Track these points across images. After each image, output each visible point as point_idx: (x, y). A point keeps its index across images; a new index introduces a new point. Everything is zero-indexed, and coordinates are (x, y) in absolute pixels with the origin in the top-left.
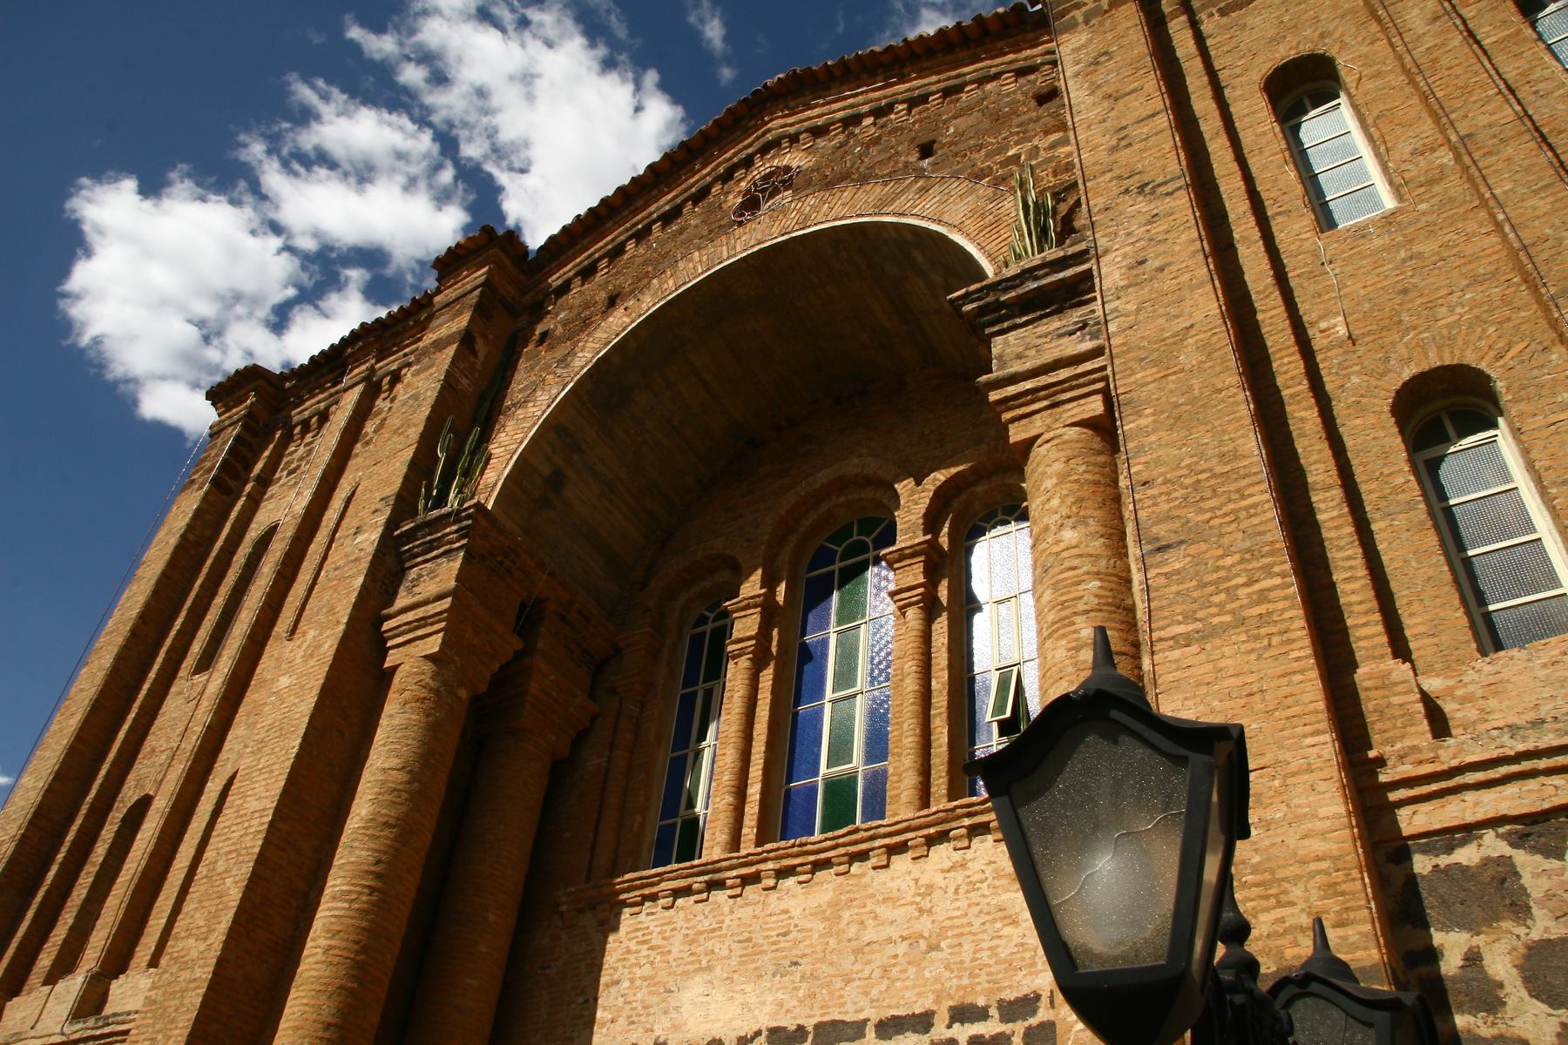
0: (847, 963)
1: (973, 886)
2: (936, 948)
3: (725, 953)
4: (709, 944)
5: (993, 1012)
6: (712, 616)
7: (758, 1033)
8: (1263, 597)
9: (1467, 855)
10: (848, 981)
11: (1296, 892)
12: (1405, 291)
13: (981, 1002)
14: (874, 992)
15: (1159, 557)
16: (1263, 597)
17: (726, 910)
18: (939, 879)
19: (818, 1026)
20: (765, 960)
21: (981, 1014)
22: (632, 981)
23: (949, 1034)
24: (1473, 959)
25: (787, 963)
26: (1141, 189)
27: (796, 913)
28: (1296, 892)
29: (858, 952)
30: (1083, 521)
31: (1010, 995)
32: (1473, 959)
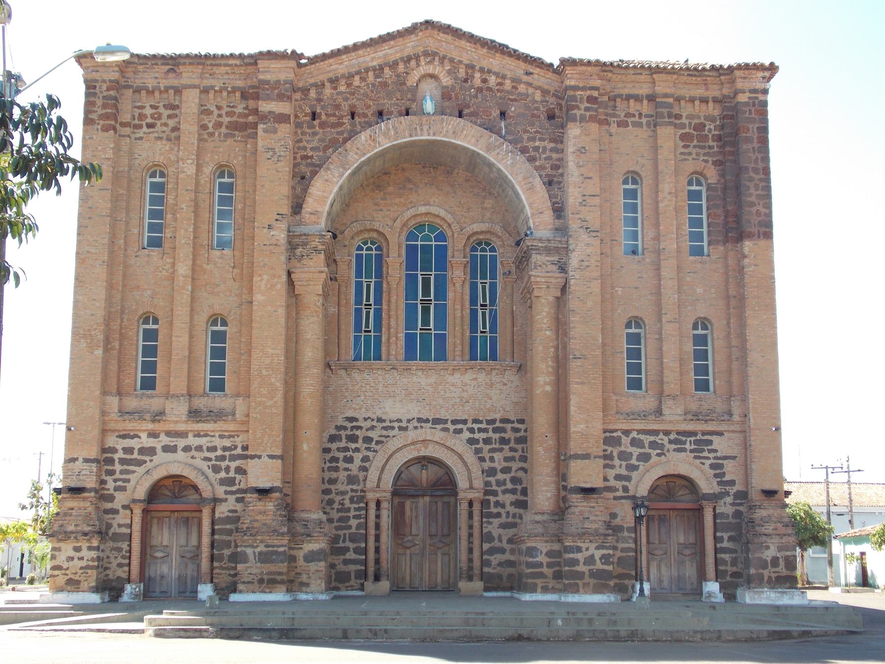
0: (441, 401)
1: (479, 386)
2: (468, 402)
3: (399, 392)
4: (393, 389)
5: (484, 422)
6: (365, 247)
7: (414, 419)
8: (594, 379)
9: (615, 434)
10: (442, 407)
11: (591, 440)
12: (636, 288)
13: (481, 419)
14: (450, 412)
15: (575, 360)
16: (594, 379)
17: (398, 378)
18: (469, 382)
19: (433, 419)
20: (413, 397)
21: (481, 422)
22: (365, 396)
23: (472, 426)
24: (612, 452)
25: (421, 399)
26: (587, 228)
27: (423, 384)
28: (591, 440)
29: (444, 399)
30: (551, 330)
31: (489, 418)
32: (612, 452)
